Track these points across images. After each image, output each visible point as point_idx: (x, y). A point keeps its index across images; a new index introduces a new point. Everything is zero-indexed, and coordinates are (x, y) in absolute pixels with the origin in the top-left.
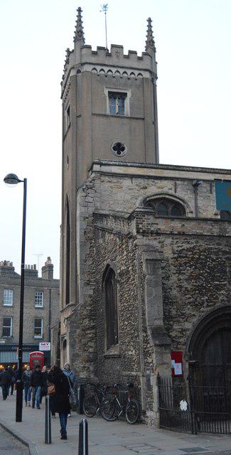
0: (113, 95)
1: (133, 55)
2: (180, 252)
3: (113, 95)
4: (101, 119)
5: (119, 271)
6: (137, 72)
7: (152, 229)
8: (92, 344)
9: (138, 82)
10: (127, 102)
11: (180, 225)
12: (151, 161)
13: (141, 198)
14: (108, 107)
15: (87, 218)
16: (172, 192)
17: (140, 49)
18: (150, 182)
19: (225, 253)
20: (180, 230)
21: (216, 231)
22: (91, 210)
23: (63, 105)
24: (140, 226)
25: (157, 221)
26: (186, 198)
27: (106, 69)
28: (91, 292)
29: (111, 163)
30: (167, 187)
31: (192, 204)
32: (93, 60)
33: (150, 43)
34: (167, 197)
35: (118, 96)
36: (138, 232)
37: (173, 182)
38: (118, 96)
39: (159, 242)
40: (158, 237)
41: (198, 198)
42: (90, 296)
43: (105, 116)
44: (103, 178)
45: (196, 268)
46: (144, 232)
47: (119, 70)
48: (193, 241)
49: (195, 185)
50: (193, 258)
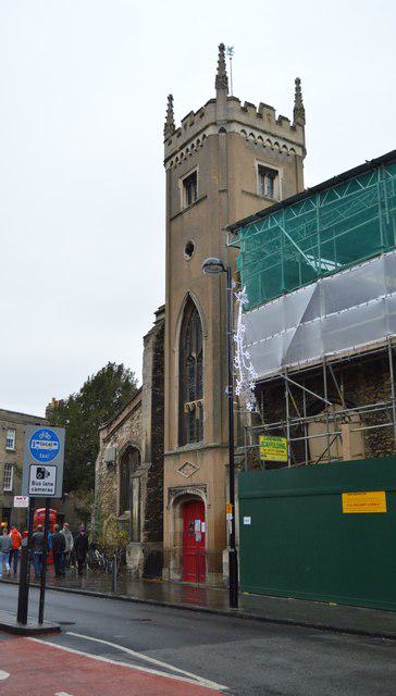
0: (263, 171)
1: (284, 122)
3: (263, 171)
6: (289, 146)
9: (290, 159)
10: (278, 182)
14: (256, 184)
17: (291, 118)
23: (169, 173)
27: (257, 134)
35: (268, 173)
38: (268, 173)
43: (256, 196)
47: (271, 138)
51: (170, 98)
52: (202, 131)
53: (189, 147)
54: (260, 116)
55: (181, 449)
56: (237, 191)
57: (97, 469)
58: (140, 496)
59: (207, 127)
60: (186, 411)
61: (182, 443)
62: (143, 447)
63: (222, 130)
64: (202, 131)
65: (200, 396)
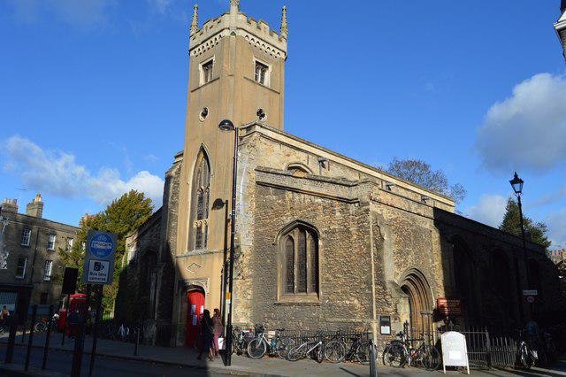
6: (277, 51)
8: (250, 292)
10: (267, 74)
13: (285, 164)
16: (305, 163)
19: (411, 226)
34: (302, 166)
37: (306, 155)
38: (261, 67)
48: (396, 213)
52: (219, 32)
55: (189, 253)
58: (156, 286)
60: (195, 226)
61: (190, 248)
62: (161, 250)
63: (233, 34)
64: (219, 32)
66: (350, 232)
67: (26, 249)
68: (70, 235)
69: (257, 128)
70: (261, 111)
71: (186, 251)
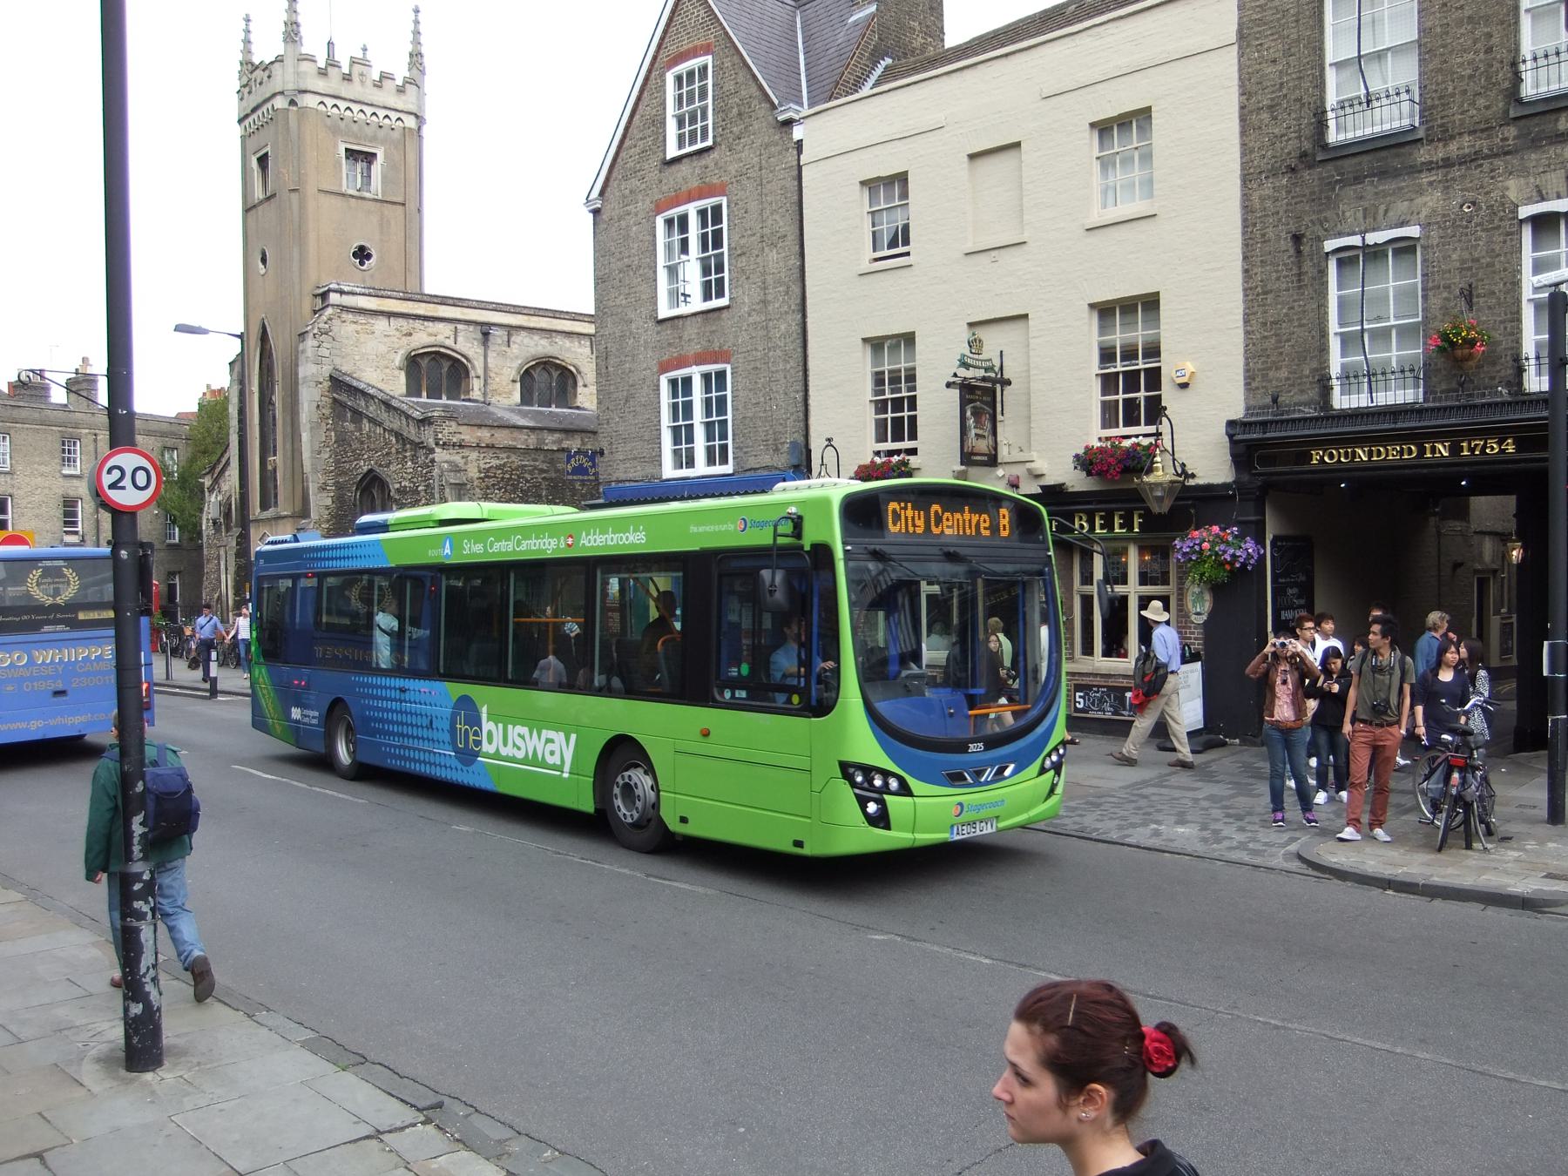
1: (387, 83)
2: (488, 470)
4: (333, 200)
5: (397, 486)
6: (394, 116)
7: (455, 440)
9: (396, 135)
10: (377, 168)
11: (489, 435)
12: (412, 287)
13: (402, 353)
15: (321, 383)
16: (450, 343)
17: (401, 72)
18: (418, 324)
19: (542, 471)
20: (489, 441)
21: (532, 440)
22: (326, 370)
24: (440, 436)
25: (462, 429)
26: (470, 353)
27: (343, 105)
28: (329, 502)
29: (358, 290)
30: (441, 335)
31: (478, 366)
32: (320, 85)
33: (416, 58)
34: (442, 350)
36: (437, 444)
37: (451, 327)
39: (463, 457)
40: (460, 451)
41: (491, 355)
42: (327, 508)
43: (343, 195)
44: (344, 316)
45: (506, 491)
46: (444, 444)
47: (365, 108)
48: (504, 455)
49: (485, 332)
50: (503, 478)
51: (248, 20)
53: (259, 112)
54: (347, 78)
56: (311, 190)
57: (204, 528)
58: (226, 569)
59: (274, 95)
60: (270, 468)
65: (275, 455)
66: (419, 493)
67: (75, 482)
68: (170, 442)
69: (334, 298)
70: (362, 249)
71: (259, 510)
